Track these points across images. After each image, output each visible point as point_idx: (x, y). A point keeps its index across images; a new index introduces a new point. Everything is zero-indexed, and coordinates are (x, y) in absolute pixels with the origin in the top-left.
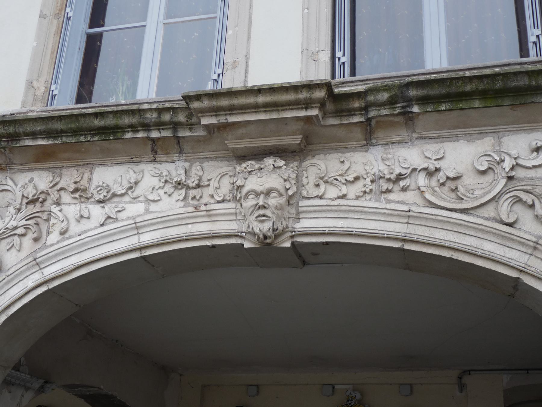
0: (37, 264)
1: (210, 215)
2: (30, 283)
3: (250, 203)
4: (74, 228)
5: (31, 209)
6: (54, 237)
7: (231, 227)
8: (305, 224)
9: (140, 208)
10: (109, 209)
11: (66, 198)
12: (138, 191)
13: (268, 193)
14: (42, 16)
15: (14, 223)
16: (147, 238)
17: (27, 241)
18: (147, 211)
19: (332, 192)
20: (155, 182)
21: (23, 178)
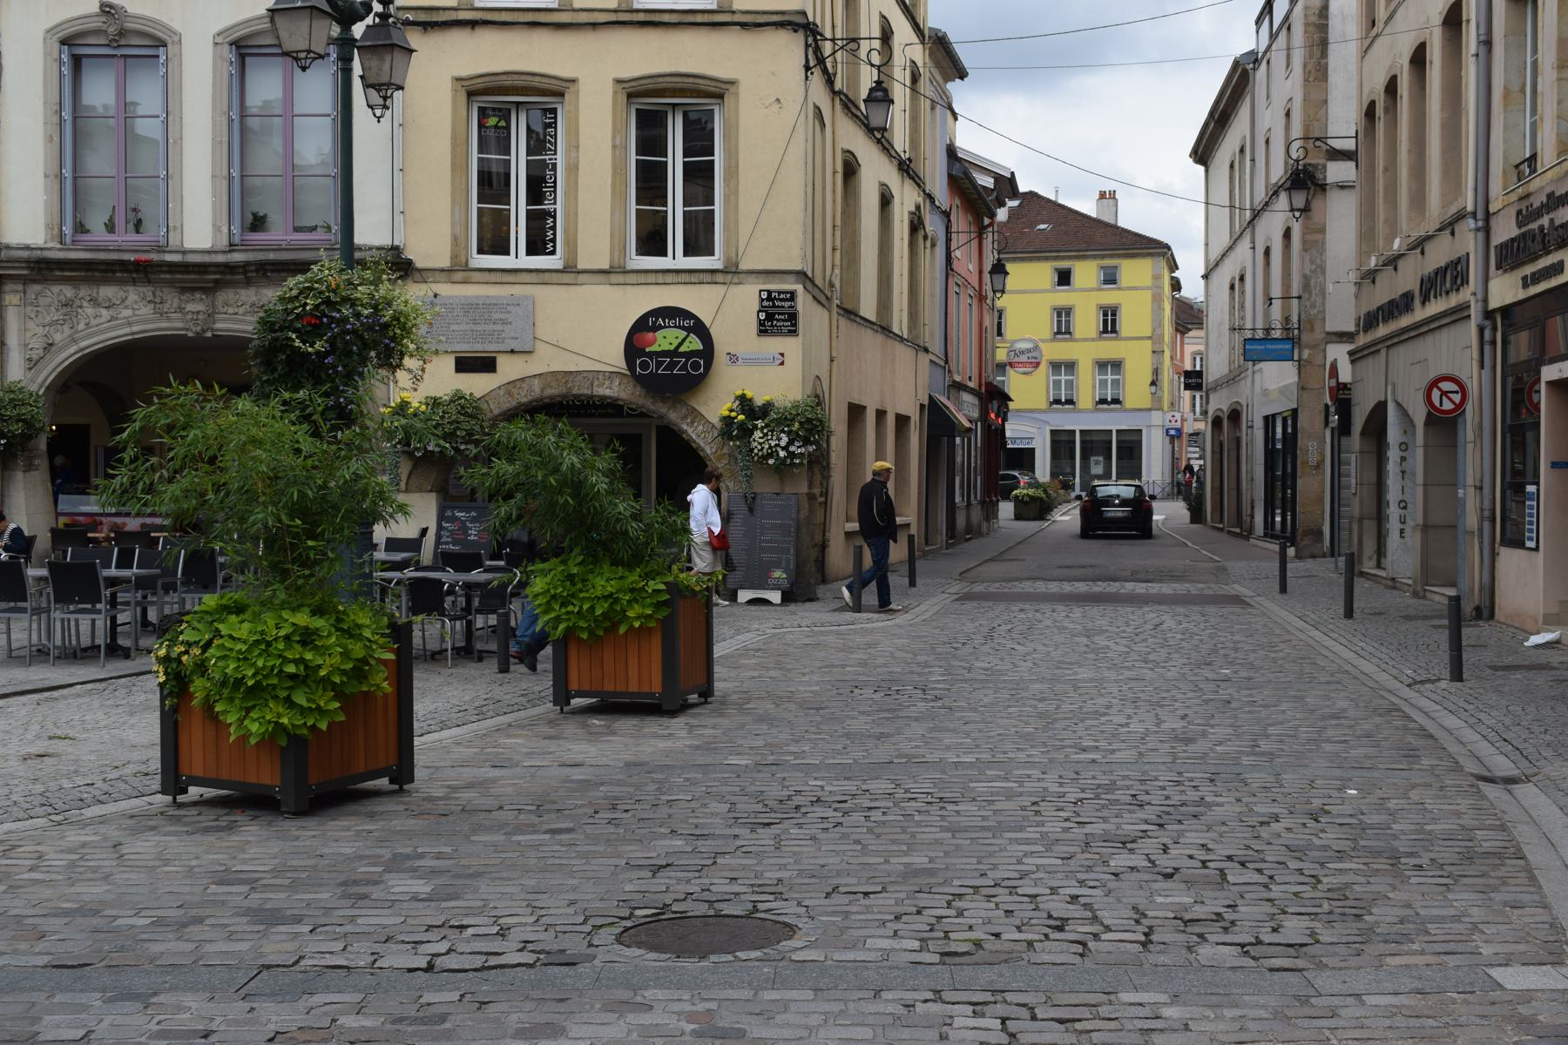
0: (75, 341)
1: (169, 319)
2: (72, 350)
3: (189, 317)
4: (93, 322)
5: (65, 310)
6: (81, 326)
7: (180, 325)
8: (218, 326)
9: (128, 312)
10: (112, 312)
11: (85, 304)
12: (127, 303)
13: (198, 312)
14: (46, 176)
15: (55, 318)
16: (135, 329)
17: (66, 328)
18: (134, 315)
19: (231, 310)
20: (136, 297)
21: (56, 289)
